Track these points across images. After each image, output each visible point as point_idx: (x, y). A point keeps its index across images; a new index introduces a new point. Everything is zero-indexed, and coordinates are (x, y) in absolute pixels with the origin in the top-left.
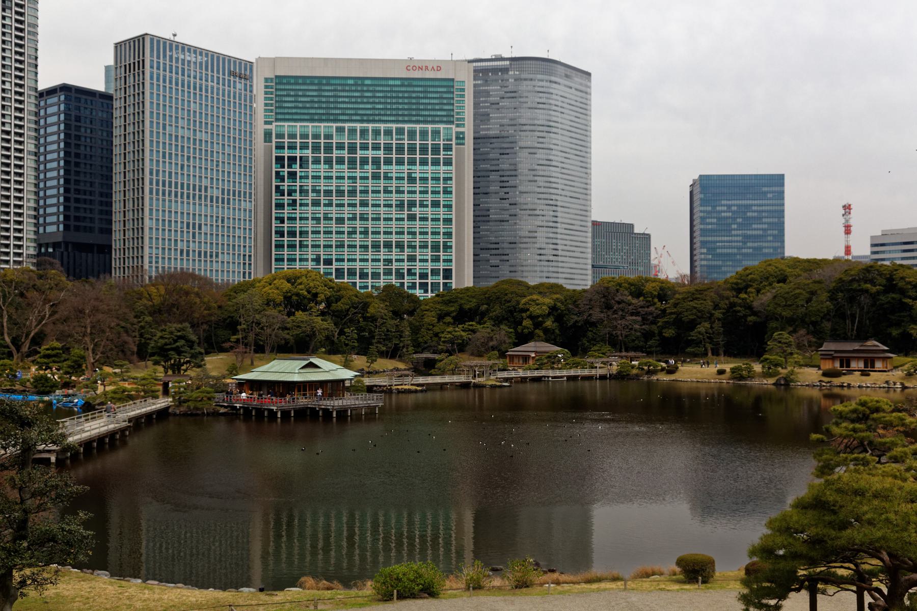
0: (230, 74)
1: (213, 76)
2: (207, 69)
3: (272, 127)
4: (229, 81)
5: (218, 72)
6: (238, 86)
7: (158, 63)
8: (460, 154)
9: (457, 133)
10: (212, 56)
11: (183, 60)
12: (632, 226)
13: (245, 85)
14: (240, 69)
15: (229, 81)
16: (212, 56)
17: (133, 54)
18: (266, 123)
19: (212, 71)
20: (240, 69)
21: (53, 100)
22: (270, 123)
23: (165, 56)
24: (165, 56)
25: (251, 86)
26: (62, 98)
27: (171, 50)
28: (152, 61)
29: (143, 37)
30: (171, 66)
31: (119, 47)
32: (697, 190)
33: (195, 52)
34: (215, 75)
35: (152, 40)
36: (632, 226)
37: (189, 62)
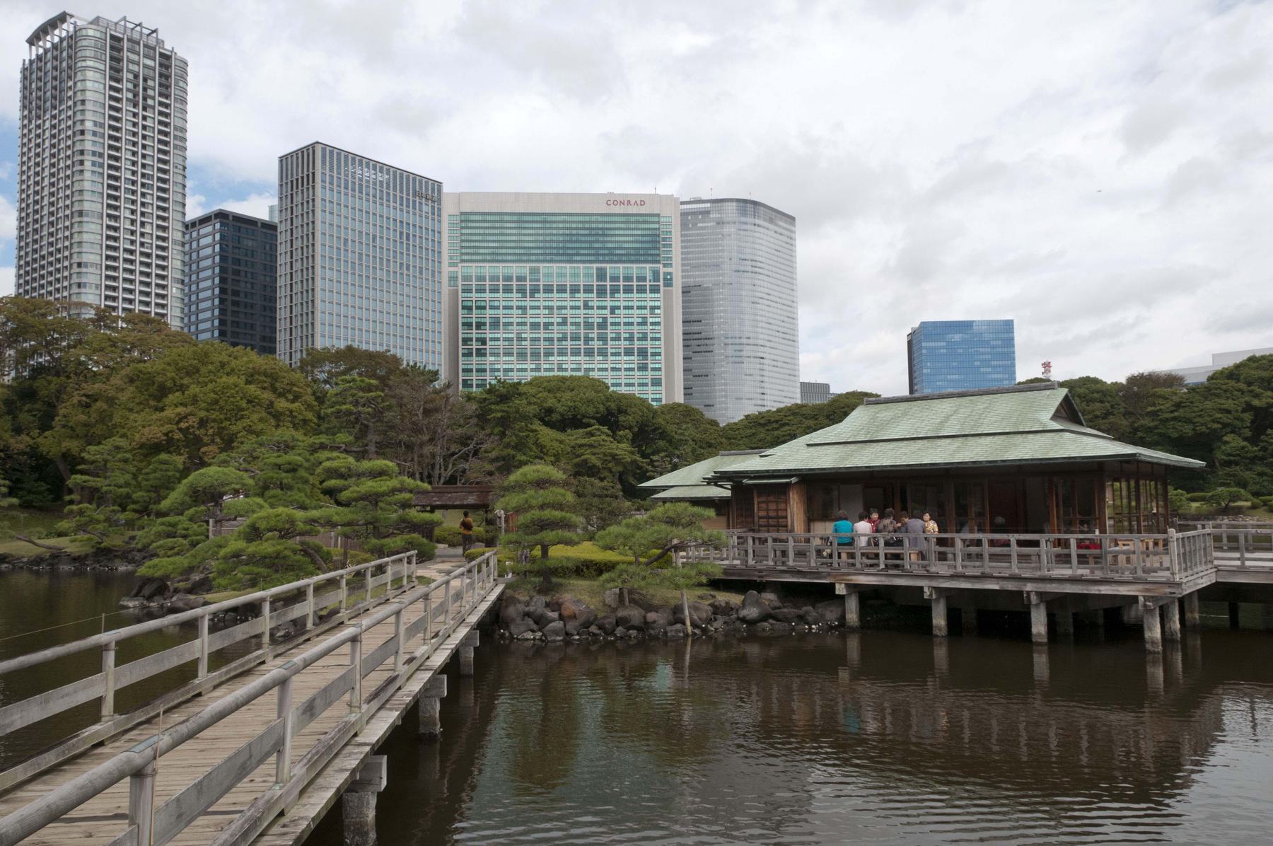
0: (414, 195)
1: (395, 196)
2: (388, 188)
4: (414, 202)
5: (401, 191)
6: (425, 208)
7: (332, 177)
8: (668, 298)
10: (395, 173)
13: (433, 207)
14: (427, 189)
15: (414, 202)
16: (395, 173)
17: (301, 170)
19: (395, 189)
20: (427, 189)
21: (207, 229)
25: (439, 210)
26: (218, 226)
28: (324, 174)
29: (313, 146)
30: (346, 181)
31: (284, 160)
33: (375, 169)
34: (398, 194)
35: (324, 150)
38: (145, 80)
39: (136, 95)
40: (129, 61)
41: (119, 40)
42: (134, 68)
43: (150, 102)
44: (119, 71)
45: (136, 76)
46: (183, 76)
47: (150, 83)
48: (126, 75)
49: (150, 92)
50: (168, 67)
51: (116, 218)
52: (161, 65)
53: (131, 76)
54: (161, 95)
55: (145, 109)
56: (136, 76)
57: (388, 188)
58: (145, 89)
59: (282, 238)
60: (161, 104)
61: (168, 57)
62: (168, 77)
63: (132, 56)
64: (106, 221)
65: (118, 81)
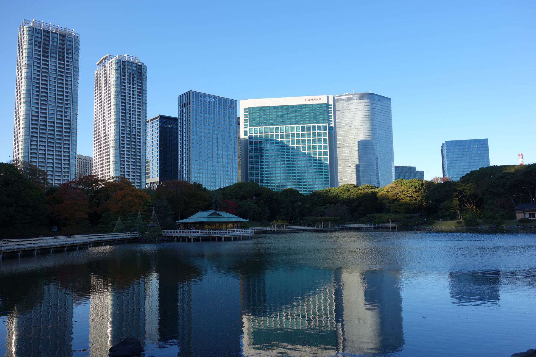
2: (216, 104)
3: (247, 129)
6: (230, 111)
9: (329, 127)
11: (206, 101)
12: (414, 168)
17: (187, 100)
18: (245, 128)
22: (247, 127)
23: (198, 100)
24: (198, 100)
27: (201, 97)
31: (180, 97)
32: (445, 148)
35: (193, 93)
36: (414, 168)
37: (209, 101)
38: (133, 75)
39: (130, 80)
40: (128, 69)
41: (125, 62)
42: (129, 71)
43: (135, 82)
44: (125, 73)
45: (130, 74)
46: (145, 72)
47: (135, 75)
48: (127, 74)
49: (135, 79)
50: (141, 69)
51: (124, 123)
52: (138, 69)
53: (129, 74)
54: (138, 79)
55: (133, 85)
56: (130, 74)
57: (216, 104)
58: (133, 78)
59: (180, 125)
60: (138, 82)
61: (141, 66)
62: (141, 73)
63: (129, 67)
64: (121, 124)
65: (125, 76)
